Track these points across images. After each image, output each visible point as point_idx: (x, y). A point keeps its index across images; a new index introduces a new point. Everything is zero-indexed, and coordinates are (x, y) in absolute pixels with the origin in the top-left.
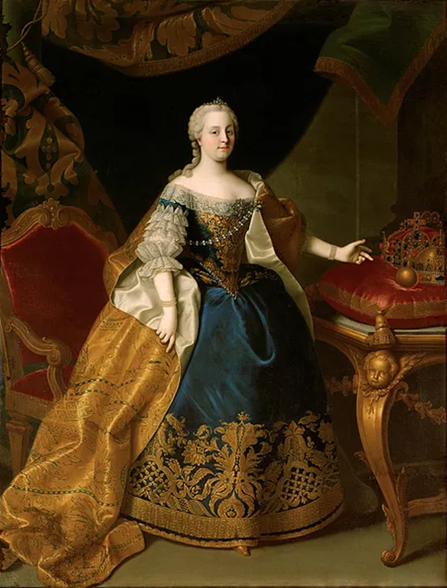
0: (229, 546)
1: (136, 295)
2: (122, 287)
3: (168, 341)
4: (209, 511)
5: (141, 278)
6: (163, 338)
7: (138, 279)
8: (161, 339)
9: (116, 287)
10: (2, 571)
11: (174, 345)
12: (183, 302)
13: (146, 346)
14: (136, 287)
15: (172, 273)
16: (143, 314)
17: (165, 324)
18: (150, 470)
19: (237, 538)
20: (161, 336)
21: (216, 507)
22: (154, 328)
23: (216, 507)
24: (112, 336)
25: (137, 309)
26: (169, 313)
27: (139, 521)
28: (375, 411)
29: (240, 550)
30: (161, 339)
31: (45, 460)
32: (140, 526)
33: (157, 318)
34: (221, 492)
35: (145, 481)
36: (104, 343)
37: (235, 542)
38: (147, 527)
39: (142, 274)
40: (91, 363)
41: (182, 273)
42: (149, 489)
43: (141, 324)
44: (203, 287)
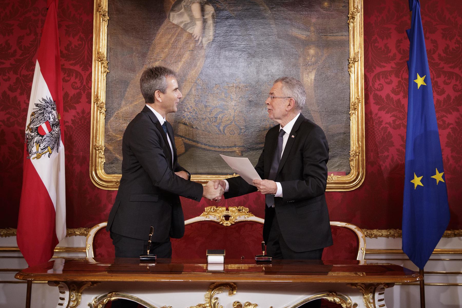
0: (231, 151)
1: (181, 15)
2: (174, 11)
3: (199, 39)
4: (220, 131)
5: (184, 6)
6: (196, 38)
7: (183, 7)
8: (194, 38)
9: (171, 11)
10: (2, 236)
11: (201, 42)
12: (206, 19)
13: (186, 43)
14: (181, 11)
15: (200, 3)
16: (186, 25)
17: (196, 29)
18: (188, 109)
19: (235, 146)
20: (195, 37)
21: (224, 130)
22: (191, 32)
23: (224, 130)
24: (169, 36)
25: (182, 22)
26: (199, 24)
27: (182, 137)
28: (310, 77)
29: (237, 153)
30: (194, 38)
31: (131, 103)
32: (182, 140)
33: (193, 27)
34: (226, 121)
35: (185, 115)
36: (164, 40)
37: (235, 148)
38: (186, 140)
39: (184, 4)
40: (157, 50)
41: (207, 3)
42: (187, 119)
43: (184, 30)
44: (217, 10)
